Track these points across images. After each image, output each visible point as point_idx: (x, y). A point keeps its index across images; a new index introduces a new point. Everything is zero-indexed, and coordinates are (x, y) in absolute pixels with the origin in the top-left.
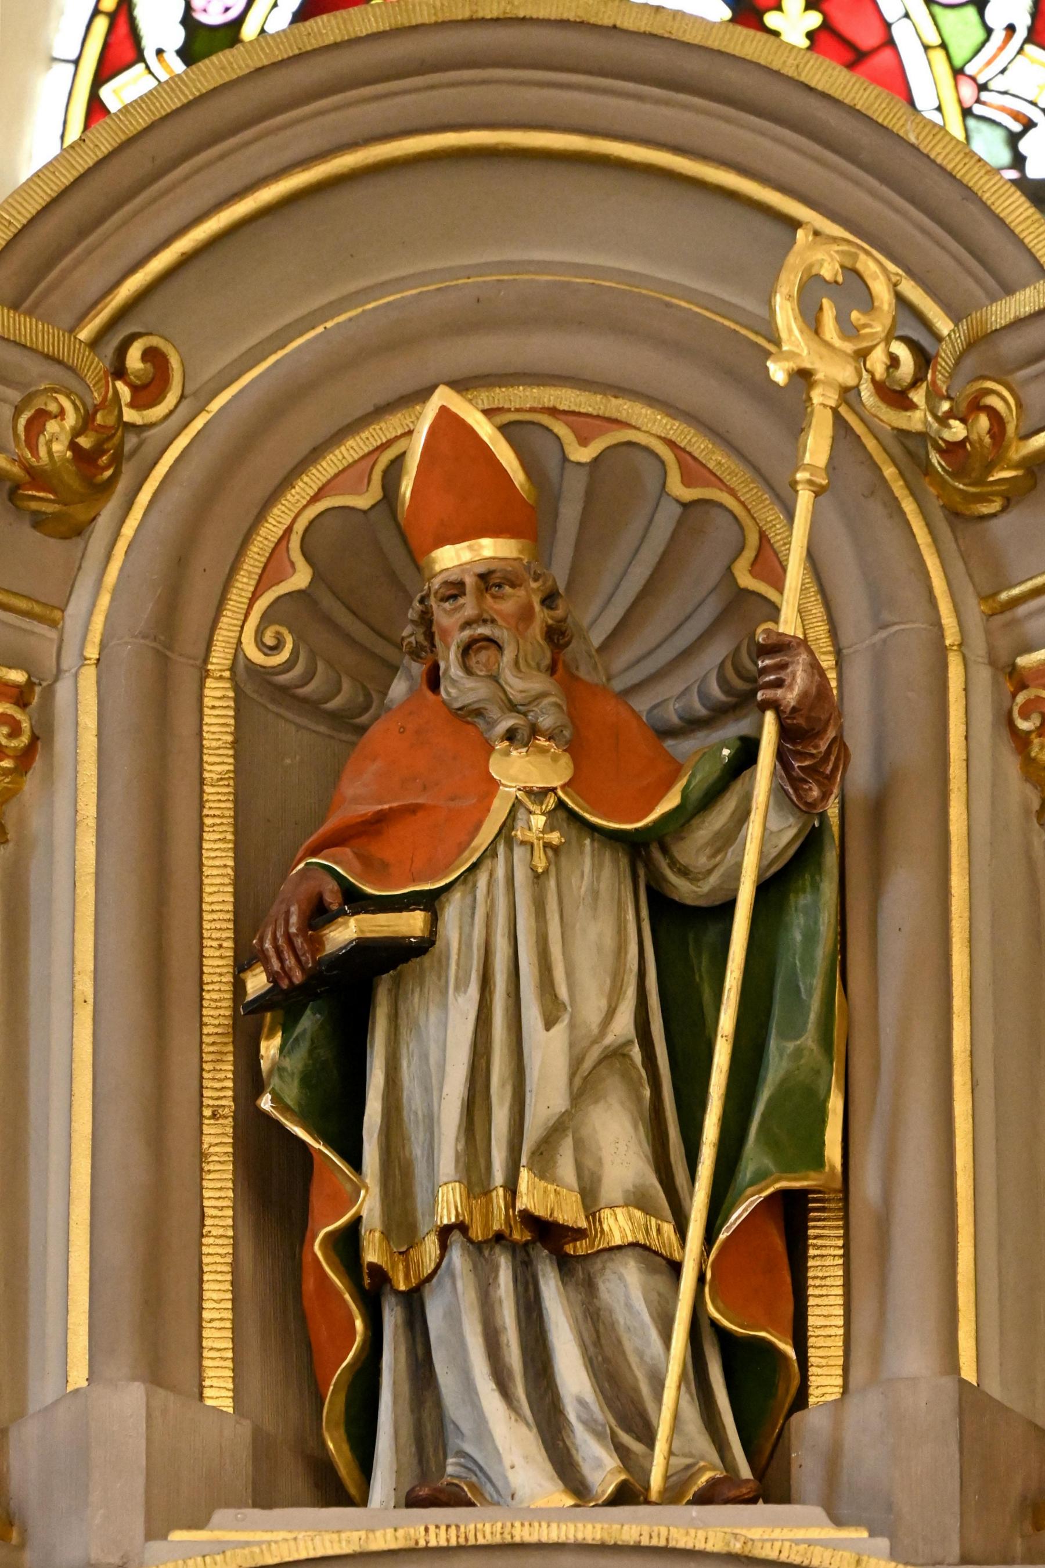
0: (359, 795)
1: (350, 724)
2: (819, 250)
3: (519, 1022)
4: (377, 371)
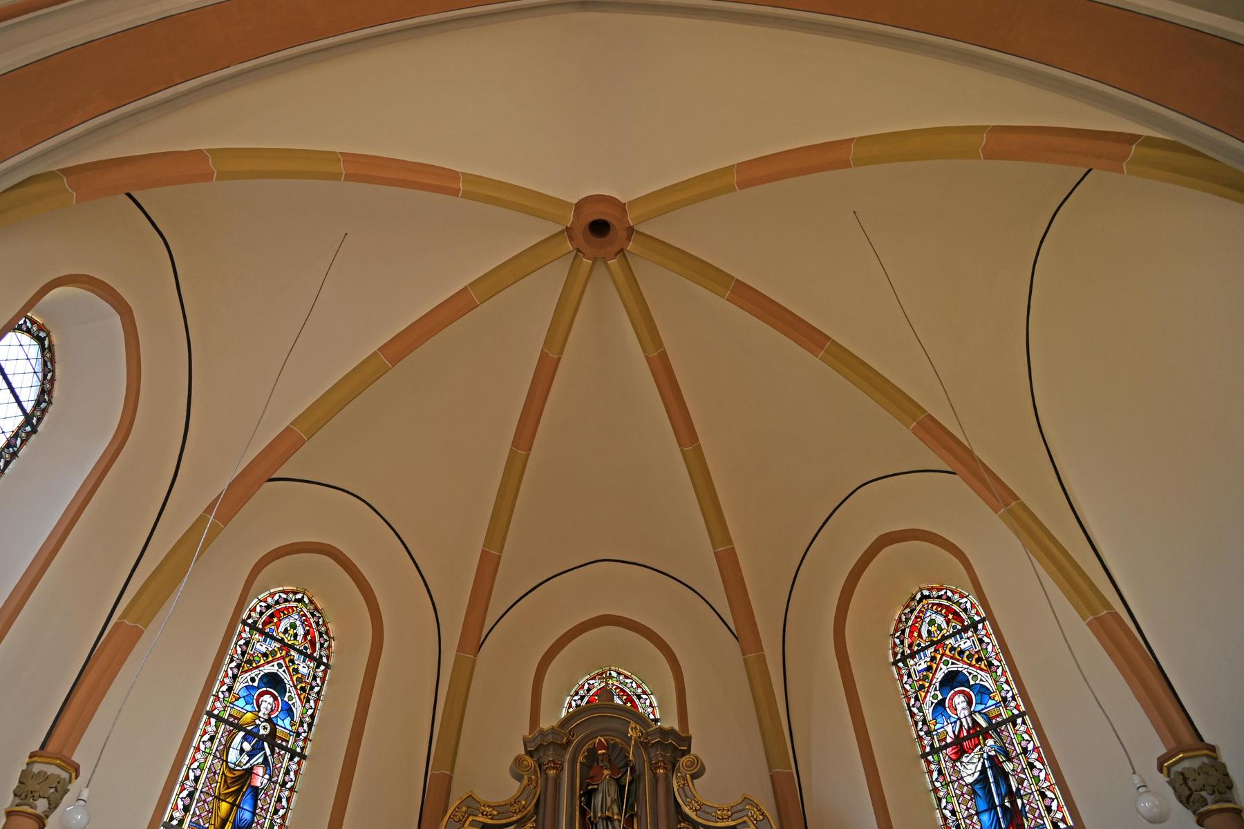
0: (591, 774)
1: (590, 767)
2: (633, 724)
3: (606, 796)
4: (592, 736)
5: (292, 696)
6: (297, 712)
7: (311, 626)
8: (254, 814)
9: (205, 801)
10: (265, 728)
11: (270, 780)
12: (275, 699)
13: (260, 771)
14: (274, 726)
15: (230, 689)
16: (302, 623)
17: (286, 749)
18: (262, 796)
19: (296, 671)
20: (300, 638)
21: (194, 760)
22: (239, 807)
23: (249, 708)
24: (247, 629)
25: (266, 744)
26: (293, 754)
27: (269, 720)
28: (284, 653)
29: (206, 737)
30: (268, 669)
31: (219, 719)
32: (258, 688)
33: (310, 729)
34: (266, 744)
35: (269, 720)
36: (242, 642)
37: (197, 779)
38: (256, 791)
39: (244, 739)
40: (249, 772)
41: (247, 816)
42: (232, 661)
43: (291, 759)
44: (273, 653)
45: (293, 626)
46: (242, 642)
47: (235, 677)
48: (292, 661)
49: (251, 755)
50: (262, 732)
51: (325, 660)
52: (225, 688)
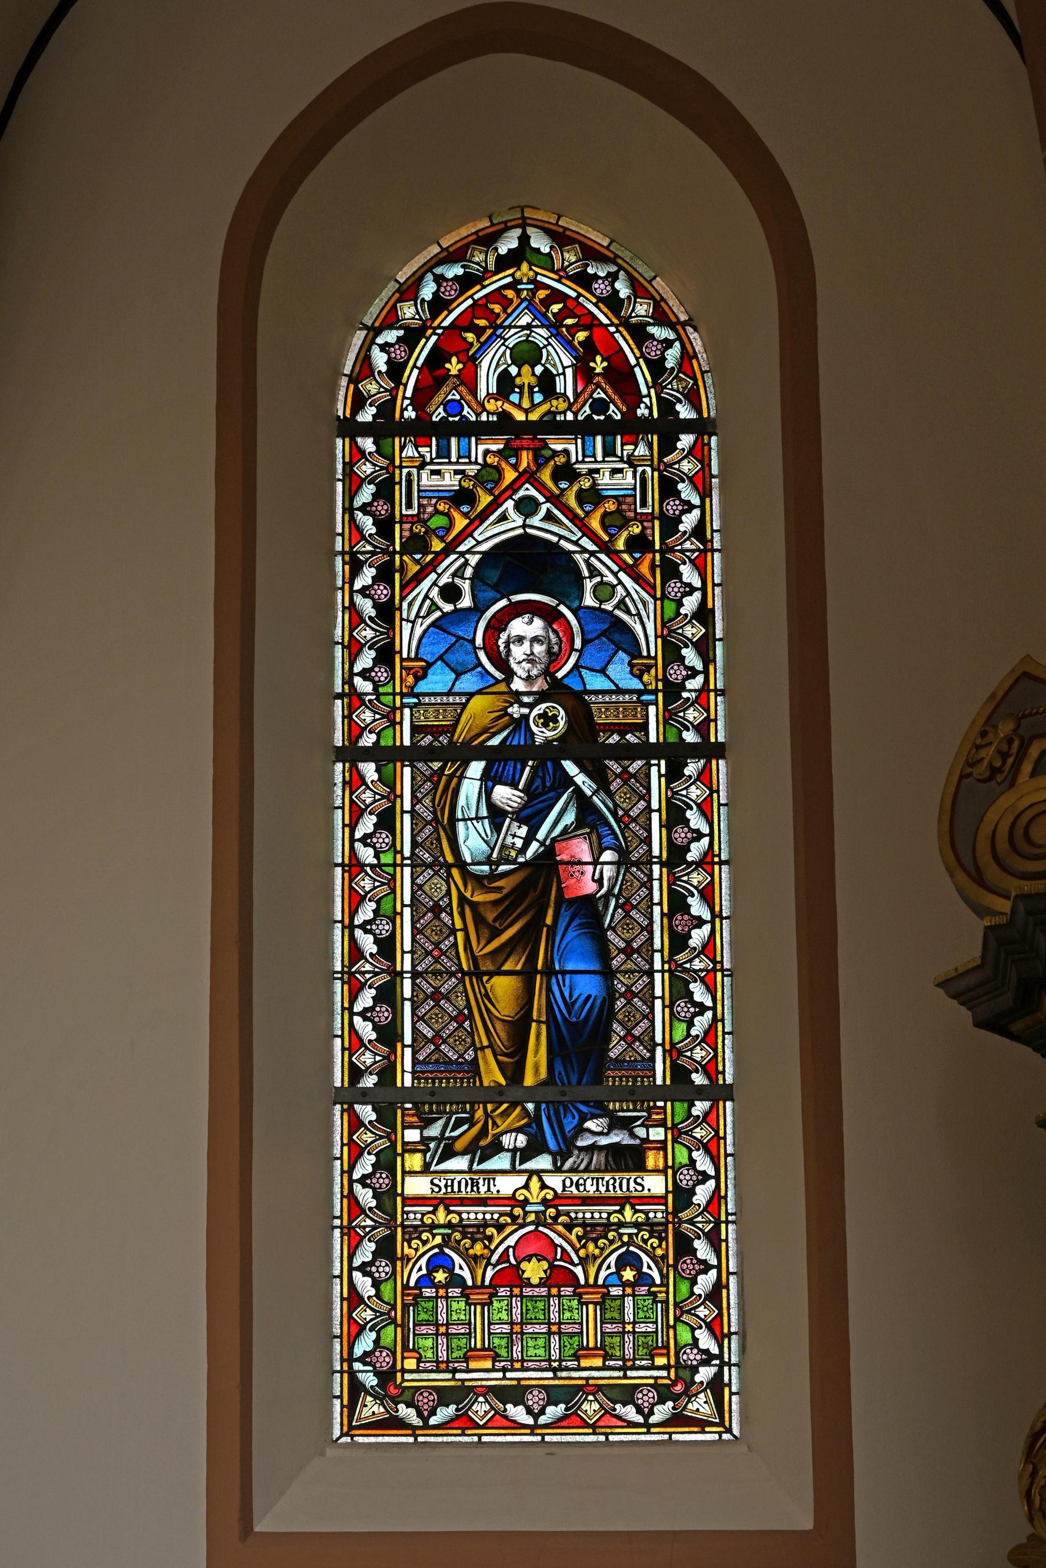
5: (612, 583)
6: (646, 631)
7: (590, 323)
8: (608, 974)
9: (436, 996)
10: (547, 719)
11: (623, 861)
12: (550, 616)
13: (582, 849)
14: (577, 702)
15: (386, 655)
16: (555, 327)
17: (648, 752)
18: (611, 914)
19: (593, 496)
20: (566, 384)
21: (355, 900)
22: (549, 972)
23: (469, 683)
24: (368, 444)
25: (570, 767)
26: (675, 756)
27: (556, 691)
28: (526, 459)
29: (367, 824)
30: (489, 535)
31: (386, 756)
32: (478, 609)
33: (708, 659)
34: (570, 767)
35: (556, 691)
36: (366, 494)
37: (387, 947)
38: (588, 909)
39: (489, 779)
40: (548, 865)
41: (588, 987)
42: (356, 567)
43: (674, 774)
44: (489, 476)
45: (527, 354)
46: (366, 494)
47: (386, 612)
48: (566, 472)
49: (531, 815)
50: (542, 734)
51: (685, 412)
52: (366, 660)
